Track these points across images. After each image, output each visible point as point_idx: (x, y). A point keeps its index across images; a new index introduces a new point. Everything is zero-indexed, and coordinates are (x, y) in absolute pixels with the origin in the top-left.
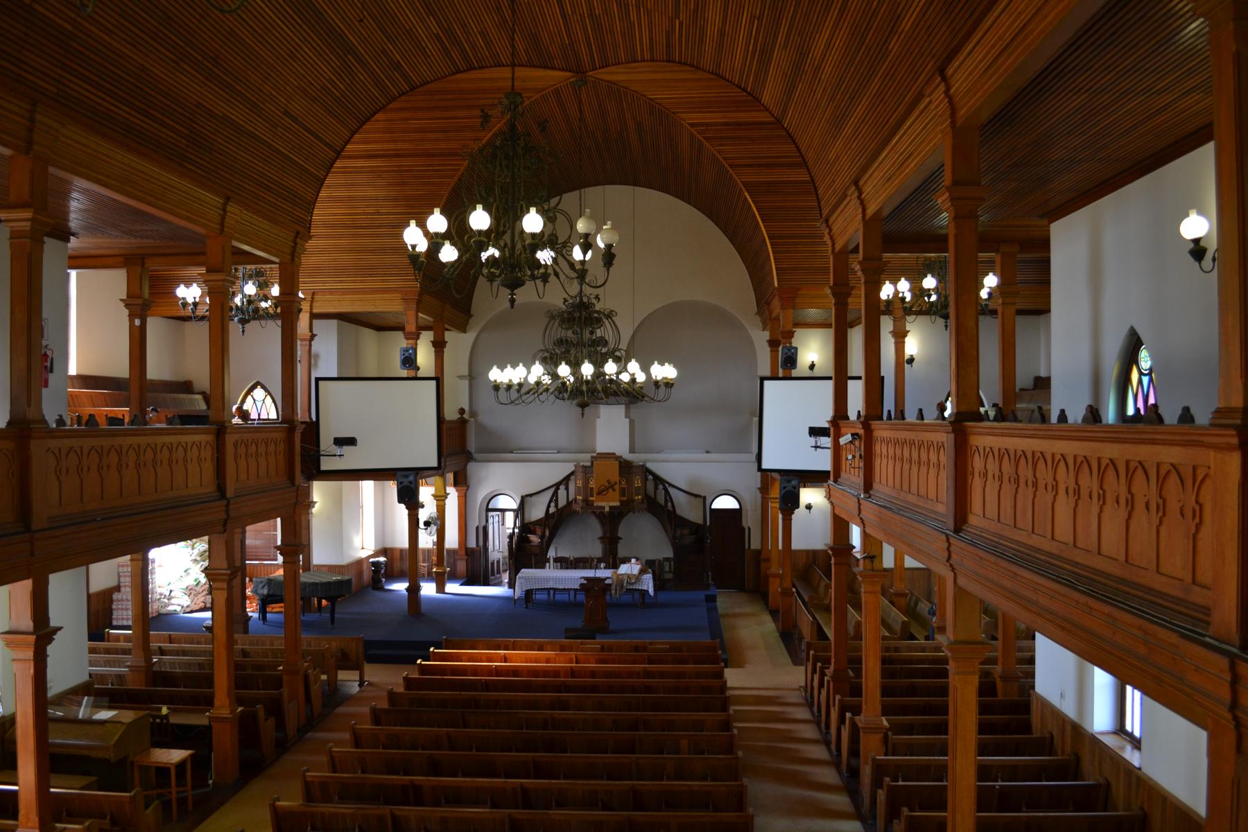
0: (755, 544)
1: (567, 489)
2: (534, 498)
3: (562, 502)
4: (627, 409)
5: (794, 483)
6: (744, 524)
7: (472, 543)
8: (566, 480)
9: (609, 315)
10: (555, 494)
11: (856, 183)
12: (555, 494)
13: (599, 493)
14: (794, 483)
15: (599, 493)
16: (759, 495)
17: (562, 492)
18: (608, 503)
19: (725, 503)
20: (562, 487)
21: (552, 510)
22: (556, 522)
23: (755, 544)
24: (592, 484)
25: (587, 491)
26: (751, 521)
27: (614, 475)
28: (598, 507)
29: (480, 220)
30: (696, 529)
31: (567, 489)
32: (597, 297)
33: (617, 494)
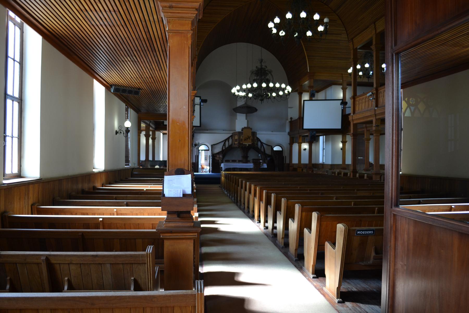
0: (288, 162)
1: (229, 142)
2: (215, 146)
3: (227, 146)
4: (246, 116)
5: (314, 133)
6: (284, 155)
7: (194, 161)
8: (228, 139)
9: (270, 72)
10: (225, 143)
11: (374, 23)
12: (225, 143)
13: (245, 140)
14: (314, 133)
15: (245, 140)
16: (289, 146)
17: (227, 143)
18: (247, 143)
19: (276, 148)
20: (227, 141)
21: (224, 148)
22: (224, 152)
23: (288, 162)
24: (241, 137)
25: (240, 140)
26: (286, 154)
27: (250, 135)
28: (245, 145)
29: (303, 15)
30: (269, 156)
31: (229, 142)
32: (266, 67)
33: (251, 141)
